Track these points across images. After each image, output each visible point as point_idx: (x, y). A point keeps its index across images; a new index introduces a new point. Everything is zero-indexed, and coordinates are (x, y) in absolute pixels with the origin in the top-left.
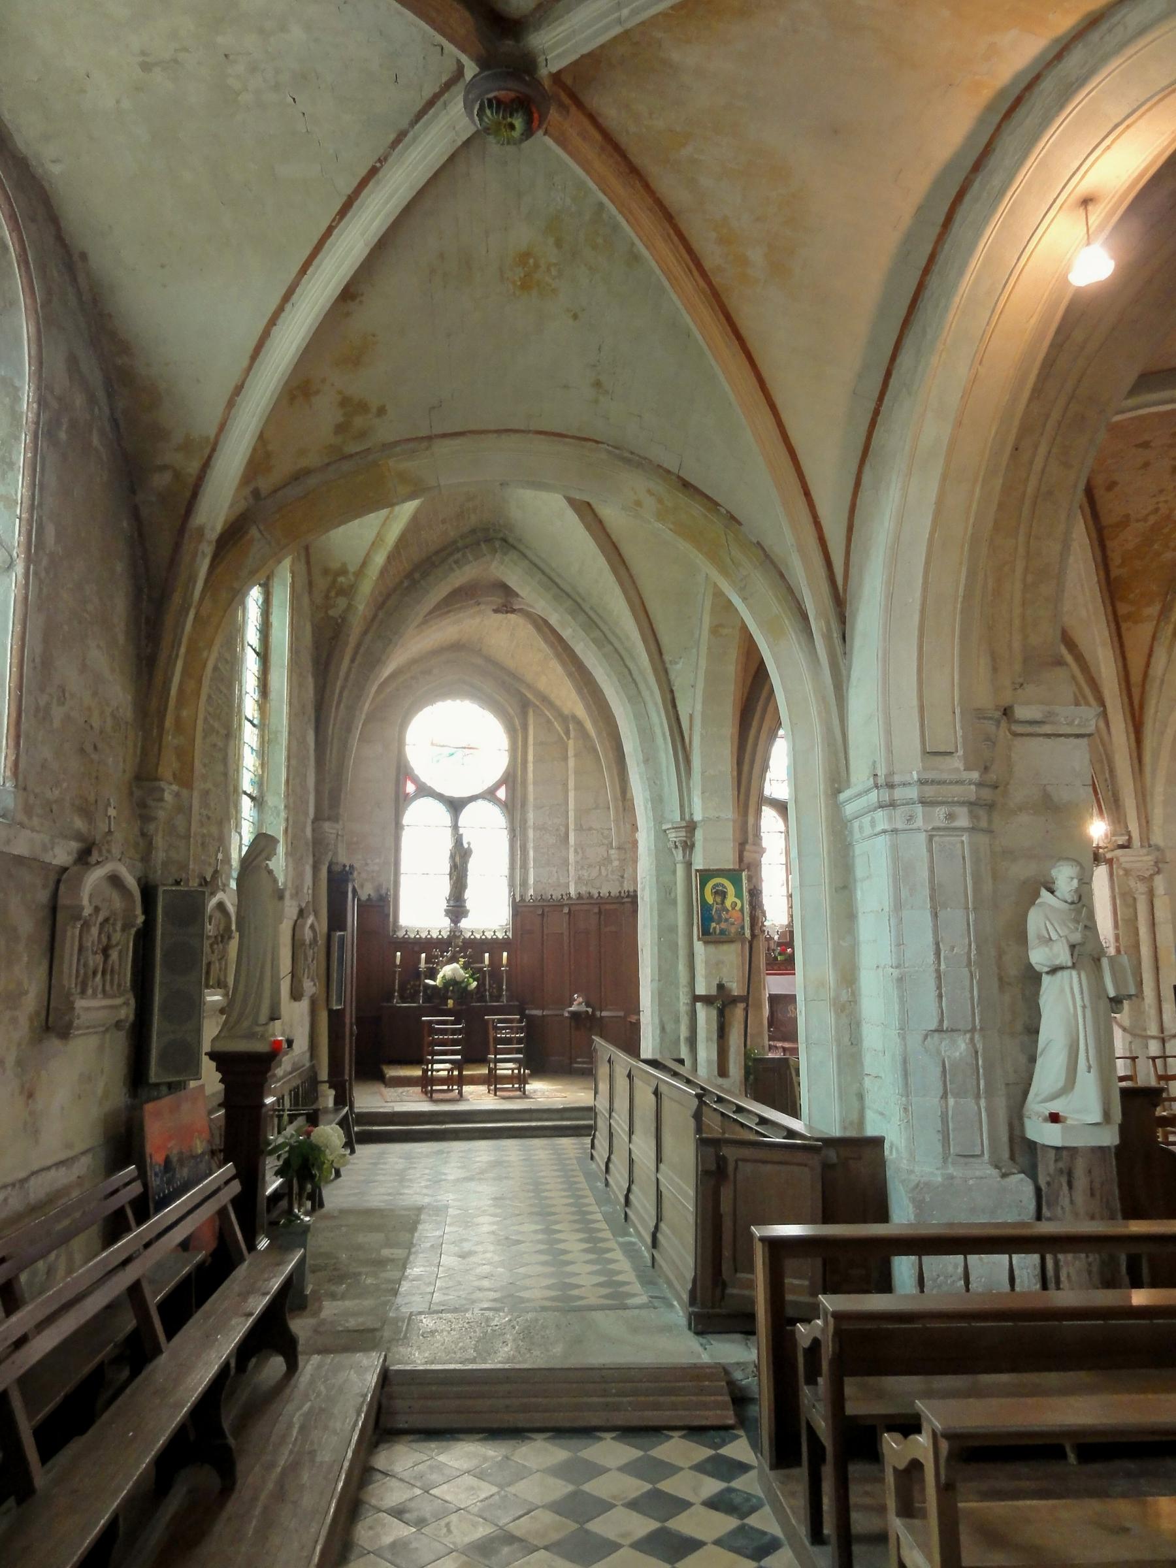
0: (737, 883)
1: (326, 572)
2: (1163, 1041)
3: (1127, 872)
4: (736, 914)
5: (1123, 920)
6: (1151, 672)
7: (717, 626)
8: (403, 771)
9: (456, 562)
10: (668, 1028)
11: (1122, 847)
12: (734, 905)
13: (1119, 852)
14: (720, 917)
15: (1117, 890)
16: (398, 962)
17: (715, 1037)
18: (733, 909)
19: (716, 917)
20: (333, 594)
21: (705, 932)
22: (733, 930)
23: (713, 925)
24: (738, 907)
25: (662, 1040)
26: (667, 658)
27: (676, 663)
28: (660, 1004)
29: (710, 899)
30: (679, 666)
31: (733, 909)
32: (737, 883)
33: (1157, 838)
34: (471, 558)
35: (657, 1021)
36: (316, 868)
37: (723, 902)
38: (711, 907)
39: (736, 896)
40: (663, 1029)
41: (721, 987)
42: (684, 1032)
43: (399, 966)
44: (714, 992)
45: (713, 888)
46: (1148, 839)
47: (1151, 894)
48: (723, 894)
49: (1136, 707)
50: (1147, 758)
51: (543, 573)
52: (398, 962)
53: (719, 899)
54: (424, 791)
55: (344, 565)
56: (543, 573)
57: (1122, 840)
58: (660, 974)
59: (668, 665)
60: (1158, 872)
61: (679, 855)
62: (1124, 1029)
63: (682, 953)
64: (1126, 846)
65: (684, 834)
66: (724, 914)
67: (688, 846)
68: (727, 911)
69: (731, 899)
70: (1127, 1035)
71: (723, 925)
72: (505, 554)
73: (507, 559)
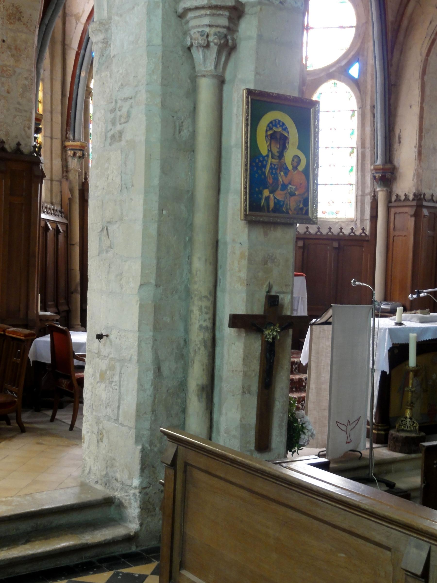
10: (165, 371)
12: (297, 160)
14: (276, 179)
17: (255, 387)
18: (295, 168)
19: (270, 181)
23: (266, 193)
24: (301, 167)
25: (156, 389)
28: (157, 327)
35: (149, 356)
37: (281, 156)
39: (299, 148)
40: (158, 371)
41: (273, 301)
42: (196, 376)
44: (258, 309)
53: (275, 150)
58: (159, 275)
61: (205, 61)
66: (282, 178)
71: (280, 195)
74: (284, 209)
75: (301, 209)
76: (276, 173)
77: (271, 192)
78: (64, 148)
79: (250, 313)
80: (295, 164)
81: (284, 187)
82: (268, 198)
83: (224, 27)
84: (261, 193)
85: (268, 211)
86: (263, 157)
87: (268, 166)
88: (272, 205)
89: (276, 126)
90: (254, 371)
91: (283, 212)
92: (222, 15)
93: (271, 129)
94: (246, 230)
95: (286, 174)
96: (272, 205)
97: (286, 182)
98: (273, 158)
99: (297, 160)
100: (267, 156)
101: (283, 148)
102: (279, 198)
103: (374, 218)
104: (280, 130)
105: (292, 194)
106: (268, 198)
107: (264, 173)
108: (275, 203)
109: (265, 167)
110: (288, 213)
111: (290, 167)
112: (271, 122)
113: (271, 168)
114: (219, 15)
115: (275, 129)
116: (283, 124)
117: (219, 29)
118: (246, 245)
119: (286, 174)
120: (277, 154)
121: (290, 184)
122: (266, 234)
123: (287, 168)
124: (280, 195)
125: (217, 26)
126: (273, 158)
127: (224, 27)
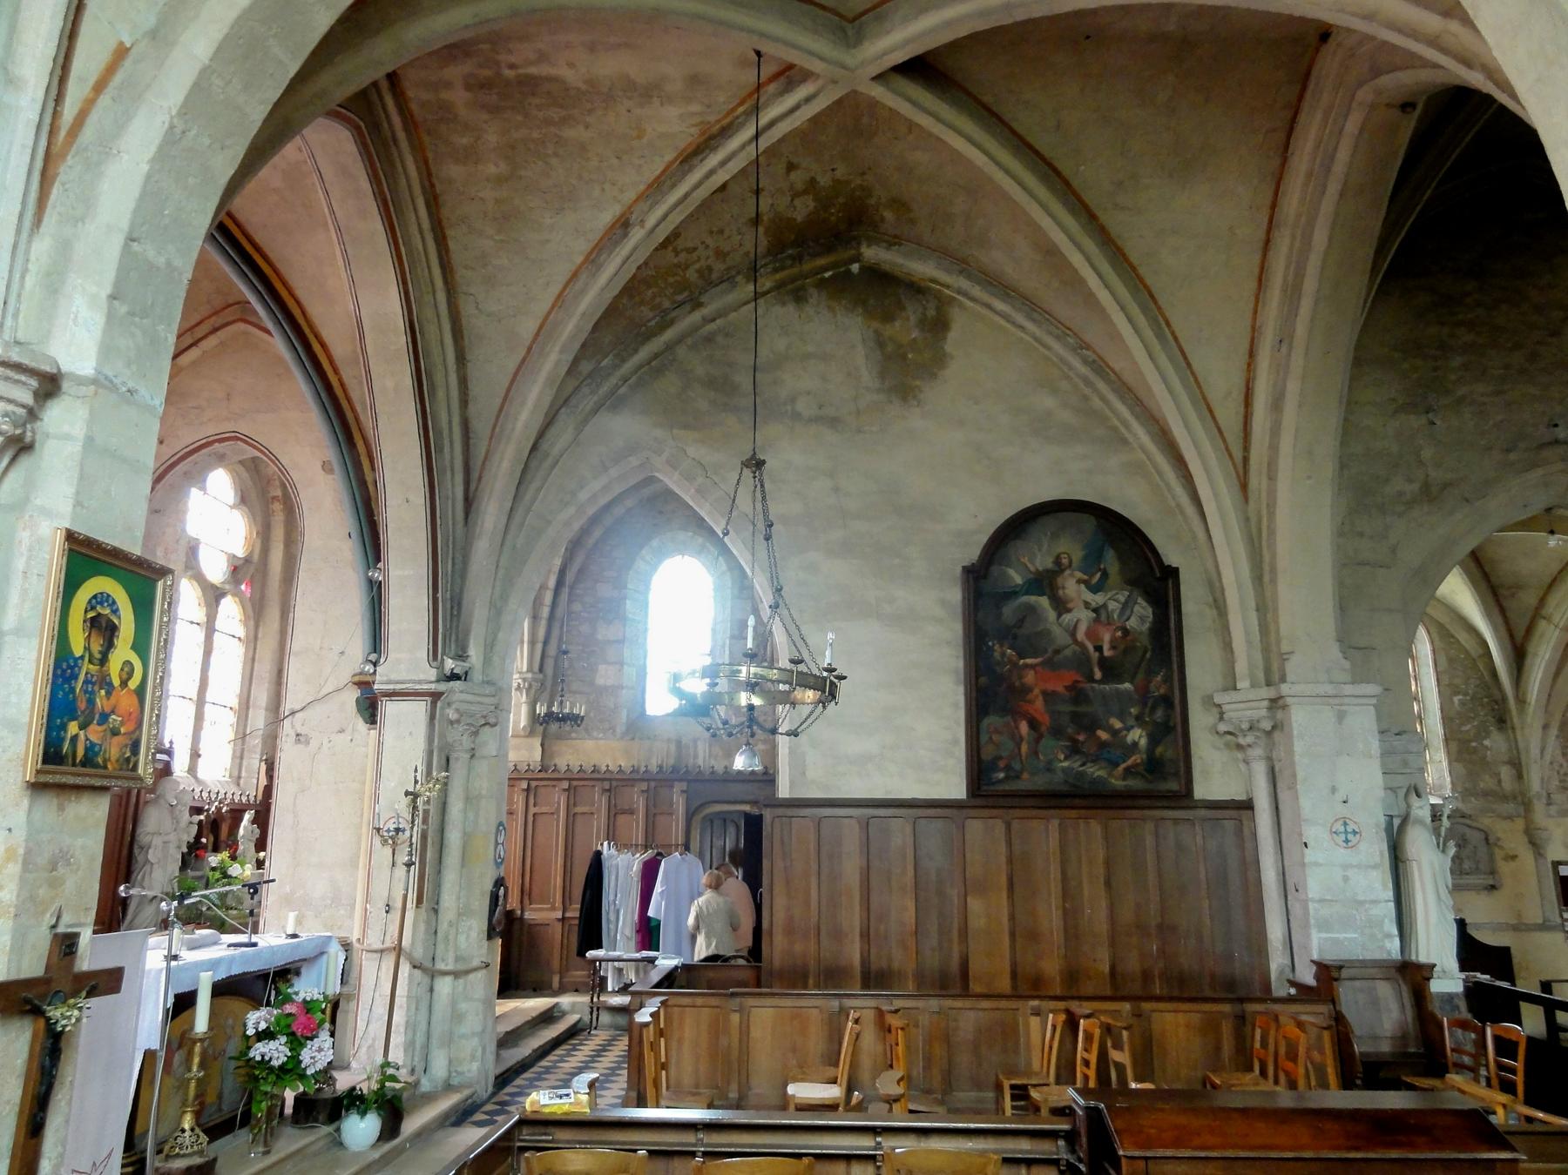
6: (544, 446)
14: (91, 702)
18: (124, 683)
19: (82, 705)
23: (73, 728)
24: (134, 683)
31: (124, 683)
37: (104, 660)
39: (134, 647)
44: (32, 966)
45: (91, 606)
53: (96, 648)
68: (110, 688)
69: (122, 652)
71: (95, 733)
74: (100, 760)
75: (128, 760)
76: (93, 693)
77: (82, 727)
79: (13, 976)
80: (125, 676)
81: (104, 718)
82: (75, 739)
83: (23, 406)
84: (64, 727)
85: (74, 765)
86: (76, 659)
87: (82, 677)
88: (80, 752)
89: (101, 603)
90: (8, 1102)
91: (96, 766)
92: (24, 384)
93: (93, 608)
94: (26, 802)
95: (109, 694)
96: (80, 752)
97: (107, 710)
98: (90, 662)
100: (82, 657)
101: (109, 645)
102: (94, 738)
104: (107, 611)
106: (75, 739)
107: (73, 690)
108: (87, 749)
109: (76, 678)
110: (105, 767)
111: (116, 682)
112: (95, 597)
113: (86, 682)
114: (17, 382)
115: (98, 608)
116: (114, 602)
117: (11, 408)
118: (20, 835)
119: (109, 694)
120: (98, 656)
121: (113, 712)
122: (61, 808)
123: (110, 684)
124: (95, 733)
125: (10, 401)
126: (90, 662)
127: (23, 406)
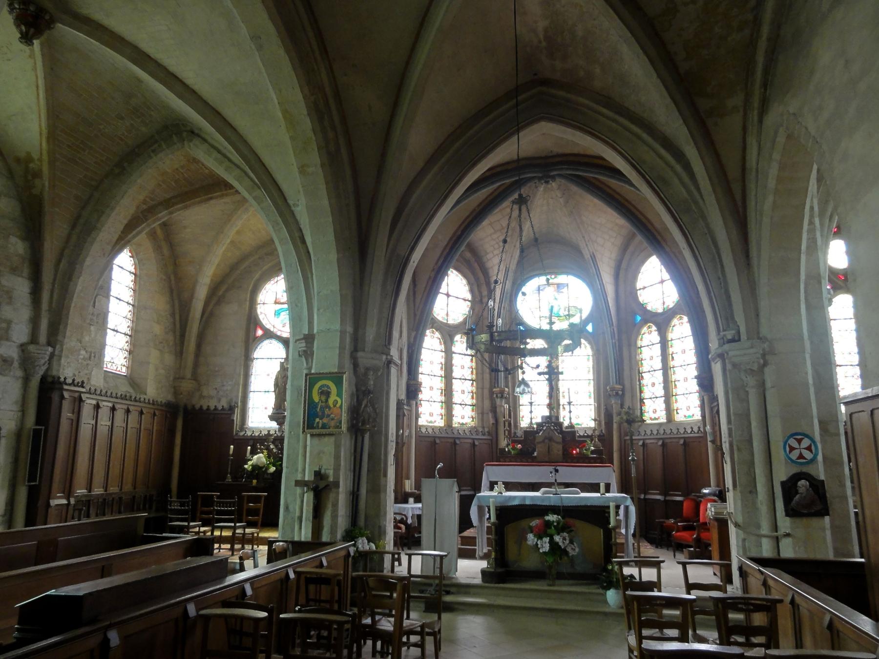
0: (338, 382)
1: (18, 160)
2: (777, 540)
3: (734, 365)
4: (336, 411)
5: (735, 414)
6: (748, 165)
7: (303, 166)
8: (253, 321)
9: (153, 151)
11: (730, 341)
12: (336, 402)
13: (727, 347)
14: (323, 413)
15: (729, 385)
16: (231, 452)
18: (335, 406)
19: (320, 414)
20: (30, 177)
21: (309, 424)
22: (332, 423)
23: (317, 420)
24: (338, 405)
26: (291, 202)
27: (298, 206)
29: (316, 398)
30: (299, 209)
31: (335, 406)
32: (338, 382)
33: (764, 331)
34: (164, 147)
36: (26, 380)
37: (327, 401)
38: (316, 405)
41: (318, 475)
43: (232, 455)
45: (320, 388)
46: (758, 333)
47: (762, 386)
48: (326, 393)
49: (740, 203)
50: (753, 252)
51: (219, 151)
52: (231, 452)
53: (323, 398)
54: (269, 335)
55: (28, 153)
56: (219, 151)
57: (729, 335)
59: (293, 208)
60: (765, 364)
62: (737, 525)
63: (301, 444)
64: (736, 340)
65: (304, 345)
66: (327, 411)
67: (307, 354)
68: (330, 408)
69: (333, 397)
70: (741, 532)
71: (325, 420)
72: (191, 141)
73: (191, 144)
78: (491, 393)
81: (328, 416)
82: (318, 423)
88: (320, 425)
99: (336, 402)
103: (703, 416)
105: (333, 419)
106: (318, 423)
124: (325, 420)
